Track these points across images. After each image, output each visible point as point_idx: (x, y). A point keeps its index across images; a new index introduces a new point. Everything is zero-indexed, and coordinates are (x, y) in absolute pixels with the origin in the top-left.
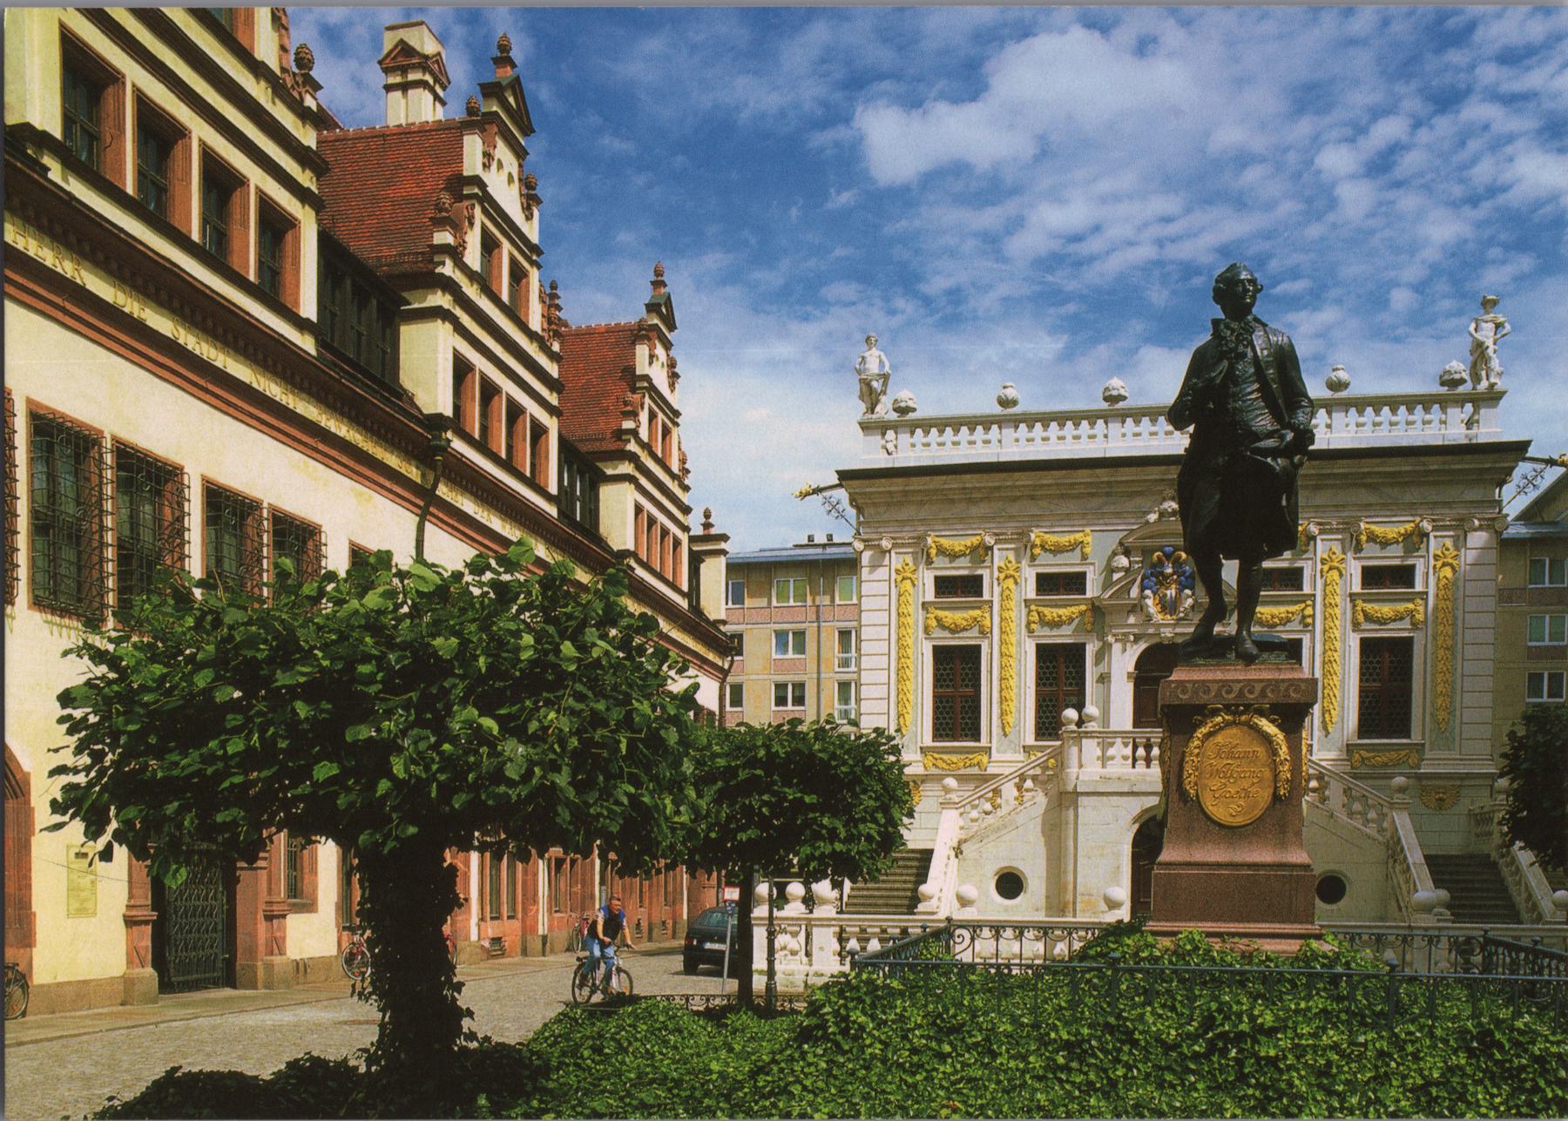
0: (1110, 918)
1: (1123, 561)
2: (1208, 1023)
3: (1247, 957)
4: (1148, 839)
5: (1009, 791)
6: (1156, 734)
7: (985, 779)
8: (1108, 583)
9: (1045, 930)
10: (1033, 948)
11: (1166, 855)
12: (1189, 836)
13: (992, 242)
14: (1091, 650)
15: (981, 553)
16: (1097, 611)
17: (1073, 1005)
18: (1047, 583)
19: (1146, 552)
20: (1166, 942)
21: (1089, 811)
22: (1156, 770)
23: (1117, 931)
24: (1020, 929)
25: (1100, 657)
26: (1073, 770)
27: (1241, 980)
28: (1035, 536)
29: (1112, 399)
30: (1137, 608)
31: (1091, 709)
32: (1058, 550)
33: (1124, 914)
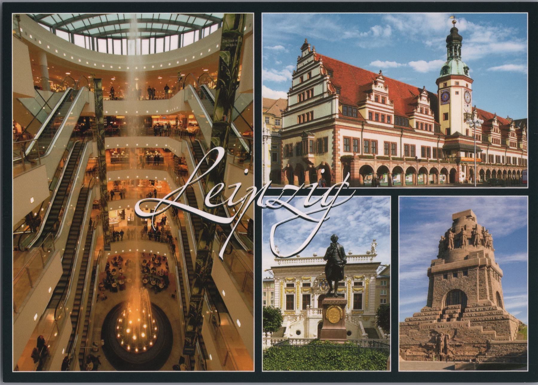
0: (315, 338)
1: (316, 281)
2: (330, 354)
3: (336, 344)
4: (320, 325)
5: (298, 318)
6: (322, 309)
7: (295, 316)
8: (314, 285)
9: (304, 340)
10: (302, 343)
11: (324, 328)
12: (327, 325)
13: (296, 231)
14: (311, 295)
15: (294, 280)
16: (312, 290)
17: (309, 352)
18: (305, 285)
19: (320, 280)
20: (323, 342)
21: (311, 321)
22: (321, 314)
23: (316, 340)
24: (300, 340)
25: (313, 296)
26: (308, 314)
27: (335, 348)
28: (302, 277)
29: (315, 256)
30: (318, 289)
31: (311, 305)
32: (306, 279)
33: (317, 337)
